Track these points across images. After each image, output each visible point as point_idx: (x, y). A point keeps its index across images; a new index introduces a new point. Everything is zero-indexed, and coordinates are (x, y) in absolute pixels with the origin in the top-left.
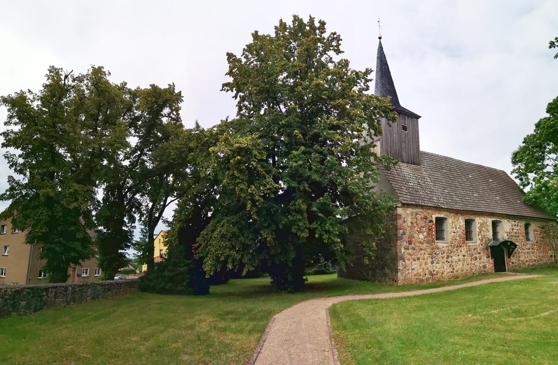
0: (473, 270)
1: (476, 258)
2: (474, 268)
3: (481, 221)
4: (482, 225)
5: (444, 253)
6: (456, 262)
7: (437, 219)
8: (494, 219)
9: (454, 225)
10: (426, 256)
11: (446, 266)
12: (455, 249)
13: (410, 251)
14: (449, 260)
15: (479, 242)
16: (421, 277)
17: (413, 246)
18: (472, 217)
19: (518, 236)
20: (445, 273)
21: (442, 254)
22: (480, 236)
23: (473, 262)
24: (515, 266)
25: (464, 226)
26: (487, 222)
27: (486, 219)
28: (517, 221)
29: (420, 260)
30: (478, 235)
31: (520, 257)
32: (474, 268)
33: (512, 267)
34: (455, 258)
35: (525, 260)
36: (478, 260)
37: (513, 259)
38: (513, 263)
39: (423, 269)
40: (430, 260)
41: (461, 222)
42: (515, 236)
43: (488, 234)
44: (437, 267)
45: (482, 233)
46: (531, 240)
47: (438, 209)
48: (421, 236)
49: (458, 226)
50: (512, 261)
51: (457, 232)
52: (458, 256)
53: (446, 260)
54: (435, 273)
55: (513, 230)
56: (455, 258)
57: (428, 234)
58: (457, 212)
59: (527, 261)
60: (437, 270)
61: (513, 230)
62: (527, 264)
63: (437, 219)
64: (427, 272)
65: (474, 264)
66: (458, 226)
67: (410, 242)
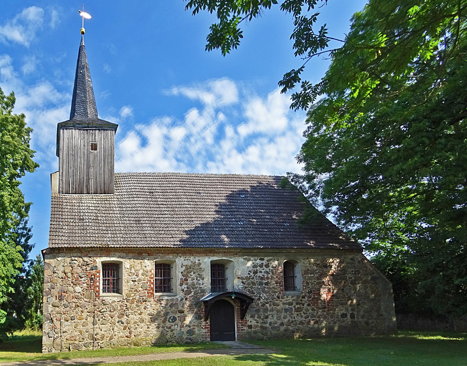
0: (168, 337)
1: (174, 319)
2: (170, 333)
3: (185, 263)
4: (188, 269)
5: (115, 310)
6: (135, 323)
7: (104, 265)
8: (215, 258)
9: (133, 271)
10: (84, 315)
11: (118, 328)
12: (134, 305)
13: (62, 309)
14: (124, 319)
15: (181, 294)
16: (77, 342)
17: (65, 302)
18: (170, 257)
19: (267, 284)
20: (116, 338)
21: (110, 311)
22: (184, 286)
23: (168, 324)
24: (255, 332)
25: (154, 272)
26: (200, 264)
27: (197, 258)
28: (266, 259)
29: (76, 320)
30: (181, 285)
31: (267, 317)
32: (170, 333)
33: (248, 333)
34: (134, 318)
35: (279, 322)
36: (177, 321)
37: (250, 320)
38: (250, 327)
39: (80, 332)
40: (90, 319)
41: (149, 265)
42: (261, 284)
43: (201, 282)
44: (102, 330)
45: (189, 281)
46: (298, 288)
47: (106, 251)
48: (78, 289)
49: (141, 272)
50: (249, 323)
51: (140, 280)
52: (140, 314)
53: (117, 320)
54: (98, 337)
55: (255, 273)
56: (134, 318)
57: (89, 286)
58: (139, 253)
59: (282, 324)
60: (103, 332)
61: (255, 273)
62: (282, 328)
63: (104, 265)
64: (86, 335)
65: (170, 328)
66: (141, 272)
67: (61, 298)
